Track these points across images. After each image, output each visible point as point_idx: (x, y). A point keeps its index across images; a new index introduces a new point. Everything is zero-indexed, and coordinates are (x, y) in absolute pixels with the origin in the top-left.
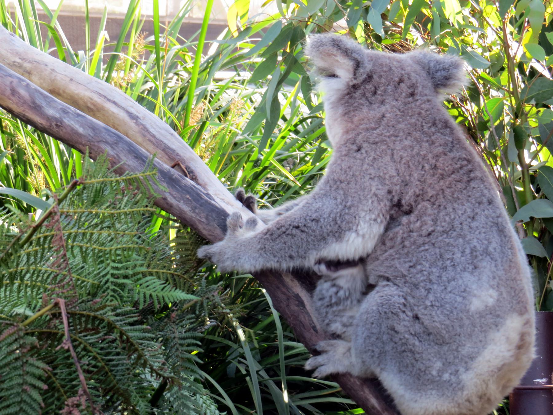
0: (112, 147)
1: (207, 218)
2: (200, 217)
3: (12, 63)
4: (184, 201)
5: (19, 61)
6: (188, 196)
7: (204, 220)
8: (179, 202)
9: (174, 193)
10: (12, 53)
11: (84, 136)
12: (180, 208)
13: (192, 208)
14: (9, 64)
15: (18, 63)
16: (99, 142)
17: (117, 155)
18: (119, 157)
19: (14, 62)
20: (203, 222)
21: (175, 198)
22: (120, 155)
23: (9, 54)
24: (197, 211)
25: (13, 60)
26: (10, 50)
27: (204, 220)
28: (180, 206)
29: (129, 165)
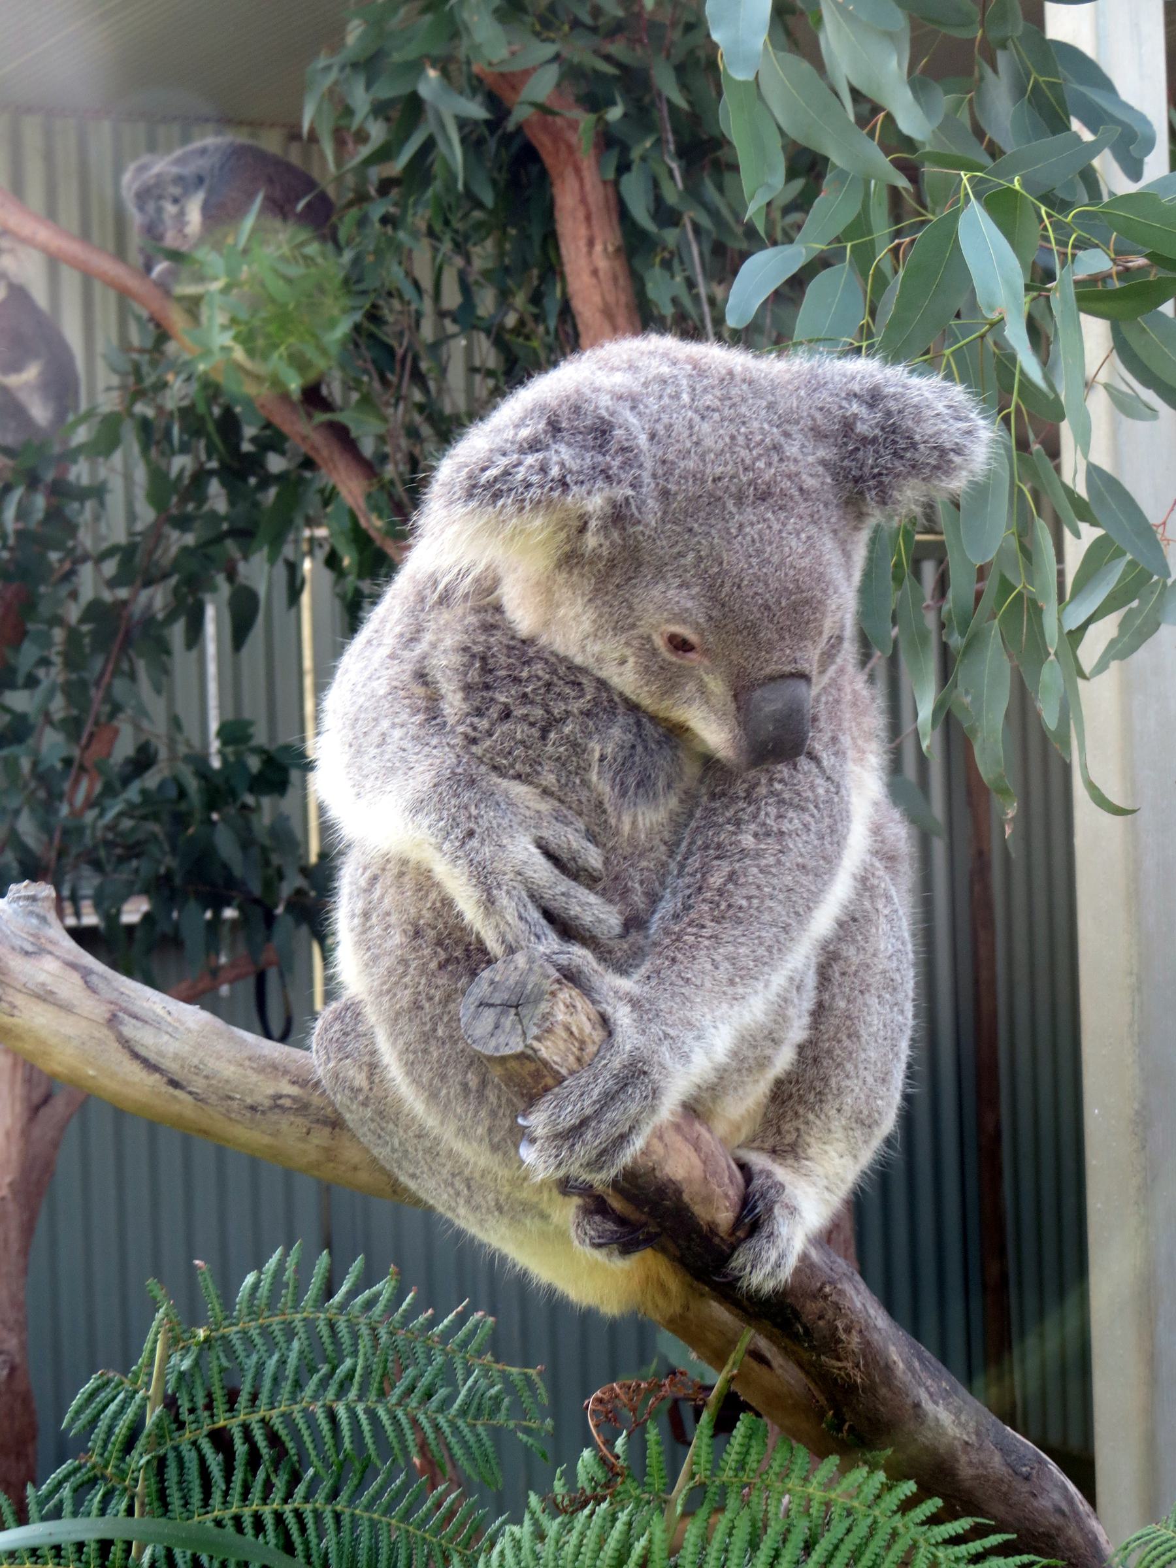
0: (856, 1288)
1: (978, 1434)
2: (968, 1433)
3: (267, 1103)
4: (944, 1399)
5: (294, 1090)
6: (944, 1384)
7: (973, 1439)
8: (936, 1403)
9: (929, 1382)
10: (261, 1070)
11: (820, 1270)
12: (937, 1420)
13: (955, 1414)
14: (253, 1108)
15: (294, 1099)
16: (840, 1279)
17: (864, 1305)
18: (867, 1311)
19: (280, 1097)
20: (971, 1445)
21: (931, 1395)
22: (868, 1306)
23: (249, 1072)
24: (963, 1418)
25: (271, 1091)
26: (250, 1059)
27: (973, 1439)
28: (939, 1416)
29: (879, 1330)
